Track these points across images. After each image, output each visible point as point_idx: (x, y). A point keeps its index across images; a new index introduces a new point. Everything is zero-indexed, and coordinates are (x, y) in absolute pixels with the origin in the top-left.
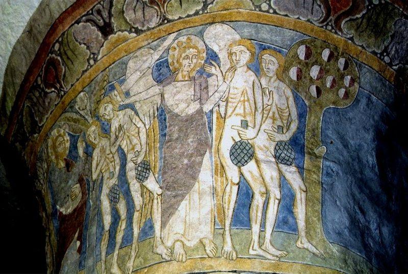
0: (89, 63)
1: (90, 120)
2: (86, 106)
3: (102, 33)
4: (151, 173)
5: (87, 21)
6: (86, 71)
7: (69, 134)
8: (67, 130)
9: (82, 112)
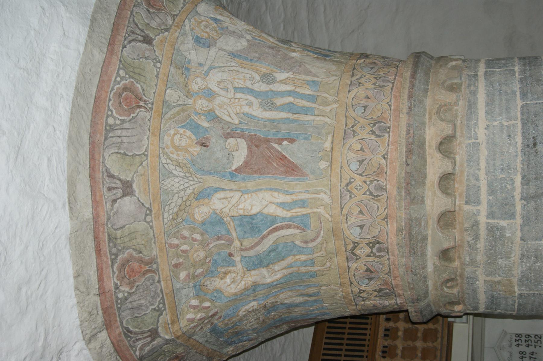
0: (157, 67)
1: (190, 102)
2: (179, 96)
3: (147, 43)
4: (274, 74)
5: (130, 42)
6: (158, 74)
7: (181, 127)
9: (179, 103)
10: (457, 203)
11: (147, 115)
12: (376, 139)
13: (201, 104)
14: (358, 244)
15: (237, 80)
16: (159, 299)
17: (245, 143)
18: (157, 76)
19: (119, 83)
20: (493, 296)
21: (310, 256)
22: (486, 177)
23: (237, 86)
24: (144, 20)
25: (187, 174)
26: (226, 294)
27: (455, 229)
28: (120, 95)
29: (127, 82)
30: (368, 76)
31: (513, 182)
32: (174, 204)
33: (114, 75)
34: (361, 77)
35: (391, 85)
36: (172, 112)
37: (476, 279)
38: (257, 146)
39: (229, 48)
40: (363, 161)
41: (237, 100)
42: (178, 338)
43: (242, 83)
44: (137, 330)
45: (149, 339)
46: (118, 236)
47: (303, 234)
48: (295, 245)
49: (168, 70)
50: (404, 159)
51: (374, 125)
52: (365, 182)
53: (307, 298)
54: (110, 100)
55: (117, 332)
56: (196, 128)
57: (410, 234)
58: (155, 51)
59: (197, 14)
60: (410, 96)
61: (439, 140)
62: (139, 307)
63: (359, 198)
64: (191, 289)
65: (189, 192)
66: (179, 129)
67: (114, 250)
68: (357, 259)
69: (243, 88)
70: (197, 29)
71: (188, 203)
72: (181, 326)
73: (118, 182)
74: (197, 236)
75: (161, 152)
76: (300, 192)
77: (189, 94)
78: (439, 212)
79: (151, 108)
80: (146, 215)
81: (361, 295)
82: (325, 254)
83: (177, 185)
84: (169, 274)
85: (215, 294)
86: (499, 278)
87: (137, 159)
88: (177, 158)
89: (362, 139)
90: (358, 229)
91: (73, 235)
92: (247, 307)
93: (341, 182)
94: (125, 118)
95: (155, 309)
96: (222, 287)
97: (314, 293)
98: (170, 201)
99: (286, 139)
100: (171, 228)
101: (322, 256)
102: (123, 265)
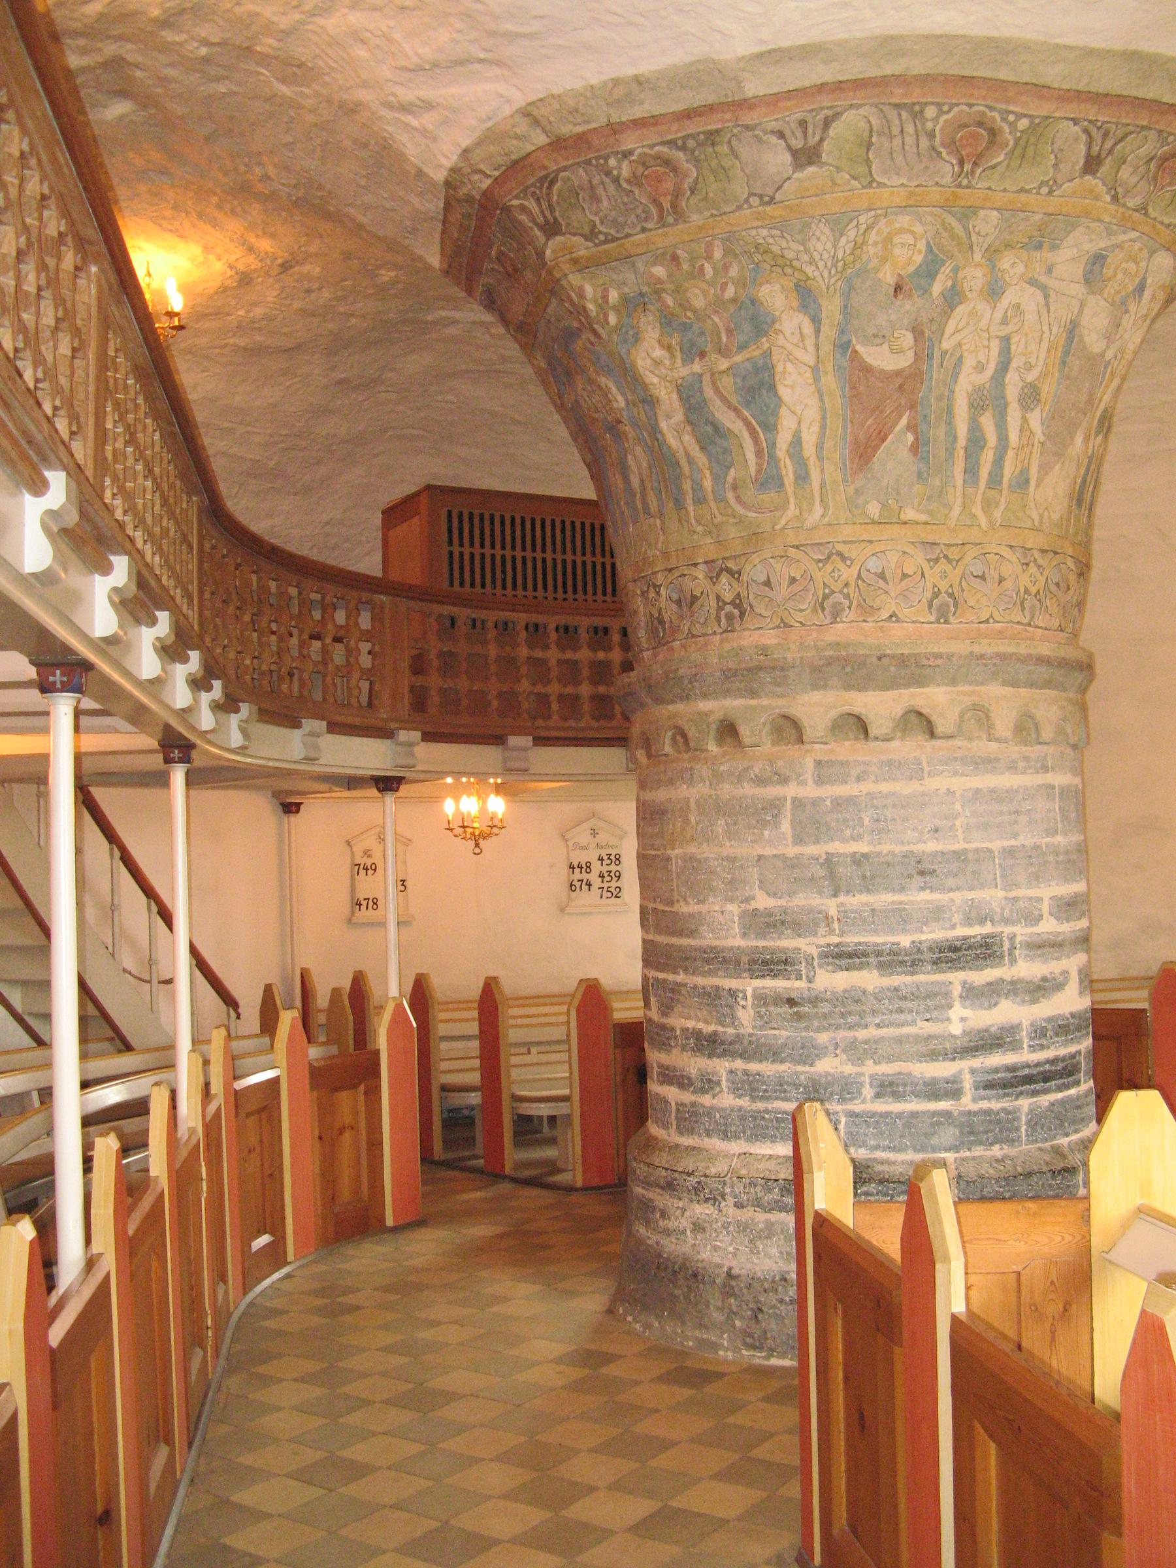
1: (978, 257)
5: (1086, 131)
6: (1028, 191)
7: (928, 244)
8: (929, 235)
10: (817, 746)
11: (948, 179)
12: (924, 600)
13: (975, 277)
14: (738, 579)
15: (1023, 340)
16: (612, 232)
17: (907, 364)
18: (1022, 190)
19: (1004, 119)
20: (663, 812)
21: (710, 497)
22: (864, 793)
23: (1014, 340)
24: (1133, 152)
25: (840, 264)
26: (633, 351)
27: (774, 744)
28: (980, 124)
29: (1007, 135)
30: (1043, 580)
31: (854, 839)
32: (784, 245)
33: (1018, 109)
34: (1039, 567)
35: (1025, 621)
36: (955, 224)
37: (691, 783)
38: (901, 387)
39: (1085, 320)
40: (884, 579)
41: (986, 343)
42: (550, 272)
43: (1019, 350)
44: (555, 198)
45: (541, 220)
46: (718, 148)
47: (748, 481)
48: (729, 468)
49: (1035, 209)
50: (888, 652)
51: (951, 595)
52: (846, 585)
53: (638, 495)
54: (970, 106)
55: (546, 163)
56: (928, 271)
57: (760, 668)
58: (1070, 181)
59: (1152, 253)
60: (1003, 657)
61: (924, 711)
62: (596, 199)
63: (818, 576)
64: (636, 289)
65: (810, 270)
66: (924, 241)
67: (691, 143)
68: (711, 578)
69: (1009, 353)
70: (1121, 255)
71: (788, 270)
72: (571, 277)
73: (817, 138)
74: (730, 292)
75: (879, 212)
76: (822, 470)
77: (992, 254)
78: (799, 715)
79: (959, 186)
80: (761, 196)
81: (652, 589)
82: (716, 521)
83: (820, 247)
84: (660, 246)
85: (631, 332)
86: (693, 821)
87: (862, 169)
88: (870, 242)
89: (923, 576)
90: (762, 578)
91: (711, 65)
92: (614, 389)
93: (844, 542)
94: (938, 139)
95: (594, 226)
96: (645, 344)
97: (648, 504)
98: (789, 237)
99: (917, 439)
100: (741, 243)
101: (713, 516)
102: (666, 162)
